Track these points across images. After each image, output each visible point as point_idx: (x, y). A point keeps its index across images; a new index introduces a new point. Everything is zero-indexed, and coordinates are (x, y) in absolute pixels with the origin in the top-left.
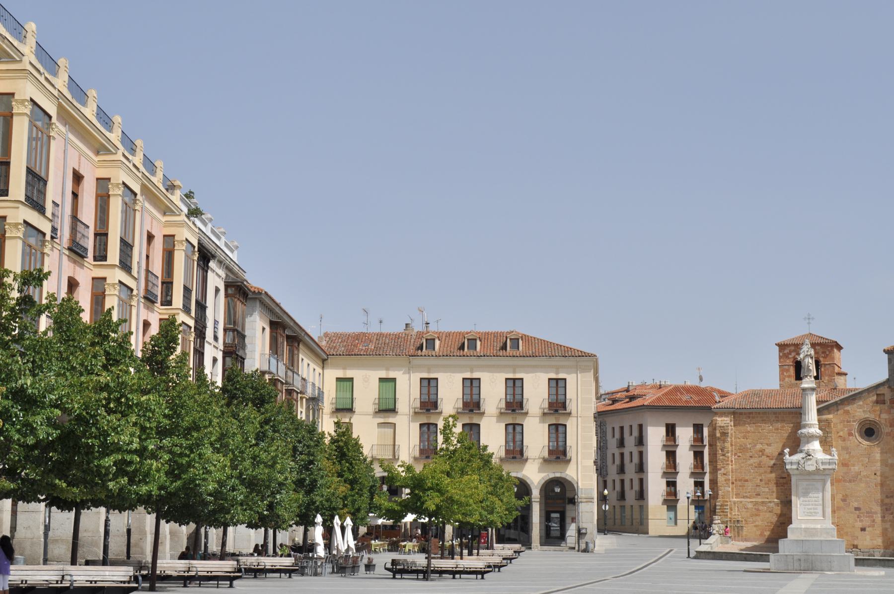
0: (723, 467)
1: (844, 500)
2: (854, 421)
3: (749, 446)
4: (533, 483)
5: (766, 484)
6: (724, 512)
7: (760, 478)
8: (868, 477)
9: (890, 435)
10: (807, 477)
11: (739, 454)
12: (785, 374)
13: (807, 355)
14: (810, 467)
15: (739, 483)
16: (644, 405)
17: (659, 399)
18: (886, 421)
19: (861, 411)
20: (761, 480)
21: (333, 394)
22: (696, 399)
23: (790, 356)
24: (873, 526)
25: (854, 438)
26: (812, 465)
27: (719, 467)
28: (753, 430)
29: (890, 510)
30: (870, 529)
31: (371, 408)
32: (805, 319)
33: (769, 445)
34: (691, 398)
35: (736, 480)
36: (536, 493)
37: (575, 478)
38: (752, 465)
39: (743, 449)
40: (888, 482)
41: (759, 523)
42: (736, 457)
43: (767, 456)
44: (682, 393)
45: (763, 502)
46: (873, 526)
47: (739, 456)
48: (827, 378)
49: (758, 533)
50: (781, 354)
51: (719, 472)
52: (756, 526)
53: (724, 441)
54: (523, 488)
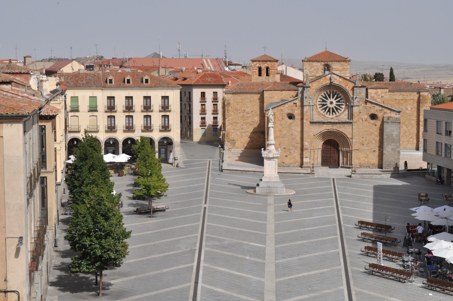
1: (279, 145)
2: (284, 114)
3: (239, 108)
4: (155, 139)
5: (246, 124)
7: (243, 122)
8: (289, 136)
11: (234, 112)
12: (254, 73)
14: (271, 156)
15: (234, 124)
16: (191, 84)
17: (198, 81)
19: (287, 109)
20: (244, 123)
21: (70, 104)
22: (214, 80)
24: (290, 155)
26: (272, 155)
27: (226, 117)
28: (241, 101)
29: (297, 148)
30: (289, 156)
31: (87, 109)
32: (263, 48)
33: (247, 108)
34: (212, 80)
35: (233, 123)
36: (157, 144)
37: (173, 138)
38: (240, 116)
39: (237, 110)
40: (296, 138)
41: (243, 141)
42: (233, 113)
43: (247, 113)
44: (208, 77)
45: (244, 132)
46: (290, 155)
47: (235, 113)
48: (272, 76)
49: (242, 145)
50: (253, 65)
51: (226, 120)
52: (241, 142)
53: (229, 106)
54: (151, 141)
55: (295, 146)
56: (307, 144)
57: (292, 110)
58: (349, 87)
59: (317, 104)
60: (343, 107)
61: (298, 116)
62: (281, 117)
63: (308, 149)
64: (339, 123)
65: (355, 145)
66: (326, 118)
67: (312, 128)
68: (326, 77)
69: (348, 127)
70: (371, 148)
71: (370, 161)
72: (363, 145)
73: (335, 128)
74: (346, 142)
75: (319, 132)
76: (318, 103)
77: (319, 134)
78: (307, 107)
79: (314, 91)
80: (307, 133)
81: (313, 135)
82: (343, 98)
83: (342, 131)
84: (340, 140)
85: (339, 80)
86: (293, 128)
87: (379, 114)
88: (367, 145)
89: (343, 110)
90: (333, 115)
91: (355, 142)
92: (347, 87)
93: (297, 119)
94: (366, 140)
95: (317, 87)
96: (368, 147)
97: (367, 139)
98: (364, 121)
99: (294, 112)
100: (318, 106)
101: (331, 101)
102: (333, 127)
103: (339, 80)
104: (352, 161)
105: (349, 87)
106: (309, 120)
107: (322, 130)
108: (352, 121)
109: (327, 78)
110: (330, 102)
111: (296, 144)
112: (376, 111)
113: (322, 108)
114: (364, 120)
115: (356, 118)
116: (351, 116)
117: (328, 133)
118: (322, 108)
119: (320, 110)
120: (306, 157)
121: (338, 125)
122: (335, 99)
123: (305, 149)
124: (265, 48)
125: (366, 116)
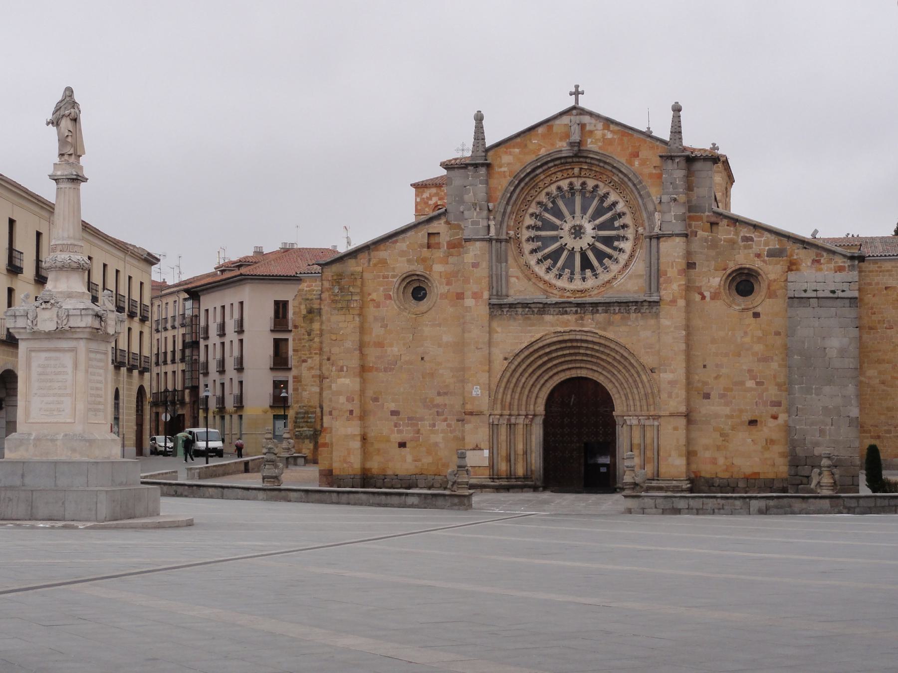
0: (310, 358)
2: (394, 276)
6: (307, 422)
9: (446, 298)
10: (46, 344)
13: (63, 115)
18: (441, 277)
23: (431, 202)
25: (393, 302)
26: (51, 320)
29: (443, 414)
40: (441, 371)
50: (418, 200)
55: (437, 406)
56: (479, 393)
57: (424, 260)
58: (643, 163)
59: (524, 238)
60: (627, 246)
61: (447, 284)
62: (382, 289)
63: (480, 414)
64: (607, 305)
65: (670, 396)
66: (555, 292)
67: (499, 329)
68: (551, 127)
69: (641, 323)
70: (741, 411)
71: (738, 461)
72: (707, 396)
73: (591, 324)
74: (637, 388)
75: (526, 344)
76: (526, 234)
77: (526, 353)
78: (478, 244)
79: (505, 182)
80: (477, 348)
81: (501, 357)
82: (625, 210)
83: (622, 341)
84: (618, 380)
85: (604, 135)
86: (427, 330)
87: (770, 267)
88: (722, 396)
89: (623, 258)
90: (584, 279)
91: (670, 382)
92: (637, 163)
93: (442, 295)
94: (717, 377)
95: (518, 167)
96: (727, 404)
97: (724, 371)
98: (708, 299)
99: (431, 270)
100: (527, 247)
101: (578, 223)
102: (583, 326)
103: (604, 135)
104: (661, 462)
105: (643, 163)
106: (486, 295)
107: (538, 336)
108: (655, 298)
109: (555, 129)
110: (574, 227)
111: (439, 394)
112: (758, 256)
113: (540, 255)
114: (707, 294)
115: (675, 286)
116: (655, 276)
117: (562, 349)
118: (540, 255)
119: (532, 260)
120: (477, 448)
121: (600, 317)
122: (594, 218)
123: (471, 414)
124: (463, 150)
125: (718, 280)
